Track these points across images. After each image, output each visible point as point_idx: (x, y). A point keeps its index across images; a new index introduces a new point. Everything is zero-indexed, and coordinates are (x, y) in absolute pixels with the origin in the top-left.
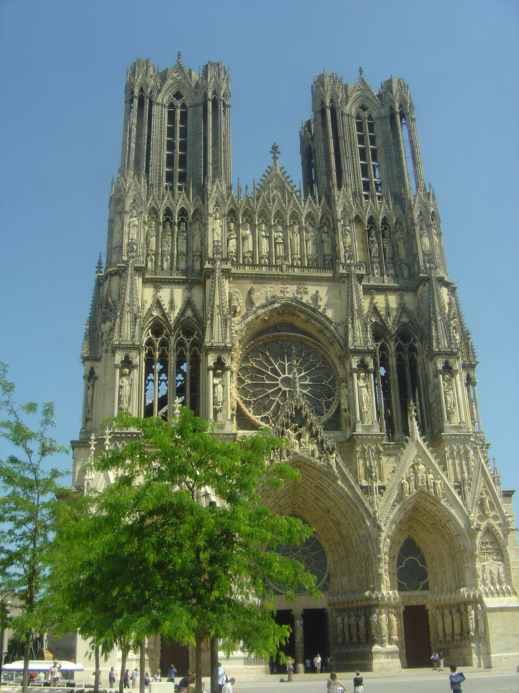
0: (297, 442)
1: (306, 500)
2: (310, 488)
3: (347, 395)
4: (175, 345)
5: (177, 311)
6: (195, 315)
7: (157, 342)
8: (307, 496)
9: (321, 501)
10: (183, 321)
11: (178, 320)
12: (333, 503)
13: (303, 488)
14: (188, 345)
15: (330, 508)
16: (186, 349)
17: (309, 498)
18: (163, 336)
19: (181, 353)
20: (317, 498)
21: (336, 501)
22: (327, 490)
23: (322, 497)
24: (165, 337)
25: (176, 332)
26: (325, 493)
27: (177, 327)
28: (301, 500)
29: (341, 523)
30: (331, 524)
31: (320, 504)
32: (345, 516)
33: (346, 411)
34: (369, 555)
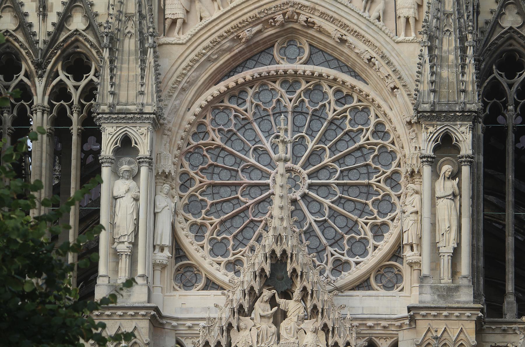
0: (274, 328)
3: (417, 213)
4: (46, 98)
5: (53, 18)
6: (90, 27)
7: (7, 89)
10: (64, 41)
11: (54, 37)
14: (75, 98)
16: (71, 106)
18: (21, 76)
19: (62, 110)
24: (26, 80)
25: (49, 67)
27: (51, 57)
33: (412, 249)
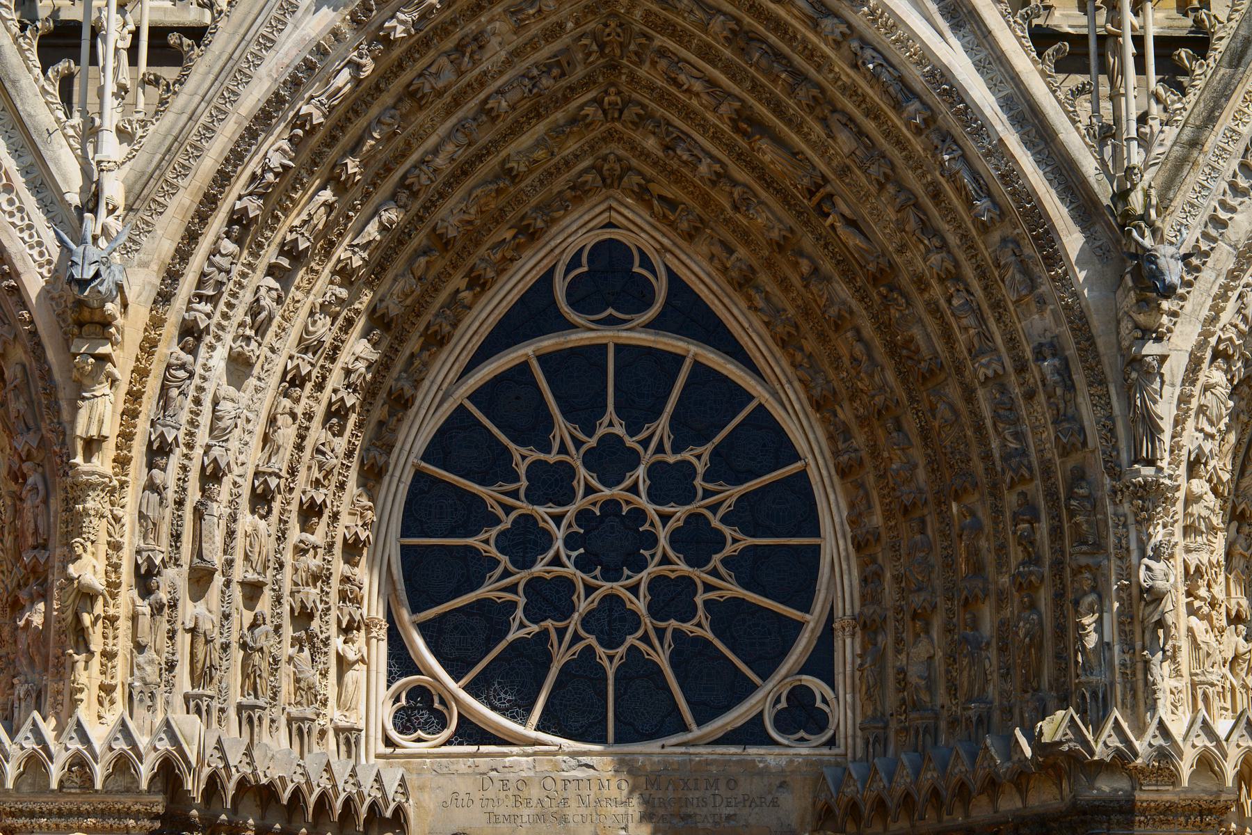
1: (684, 137)
2: (706, 52)
8: (688, 114)
9: (779, 141)
12: (845, 142)
13: (662, 52)
15: (836, 185)
17: (704, 127)
20: (746, 122)
21: (870, 126)
22: (811, 54)
23: (778, 109)
26: (799, 76)
28: (651, 143)
29: (905, 279)
30: (842, 290)
31: (768, 153)
32: (926, 227)
34: (1079, 476)
